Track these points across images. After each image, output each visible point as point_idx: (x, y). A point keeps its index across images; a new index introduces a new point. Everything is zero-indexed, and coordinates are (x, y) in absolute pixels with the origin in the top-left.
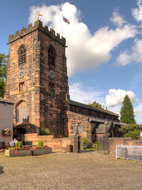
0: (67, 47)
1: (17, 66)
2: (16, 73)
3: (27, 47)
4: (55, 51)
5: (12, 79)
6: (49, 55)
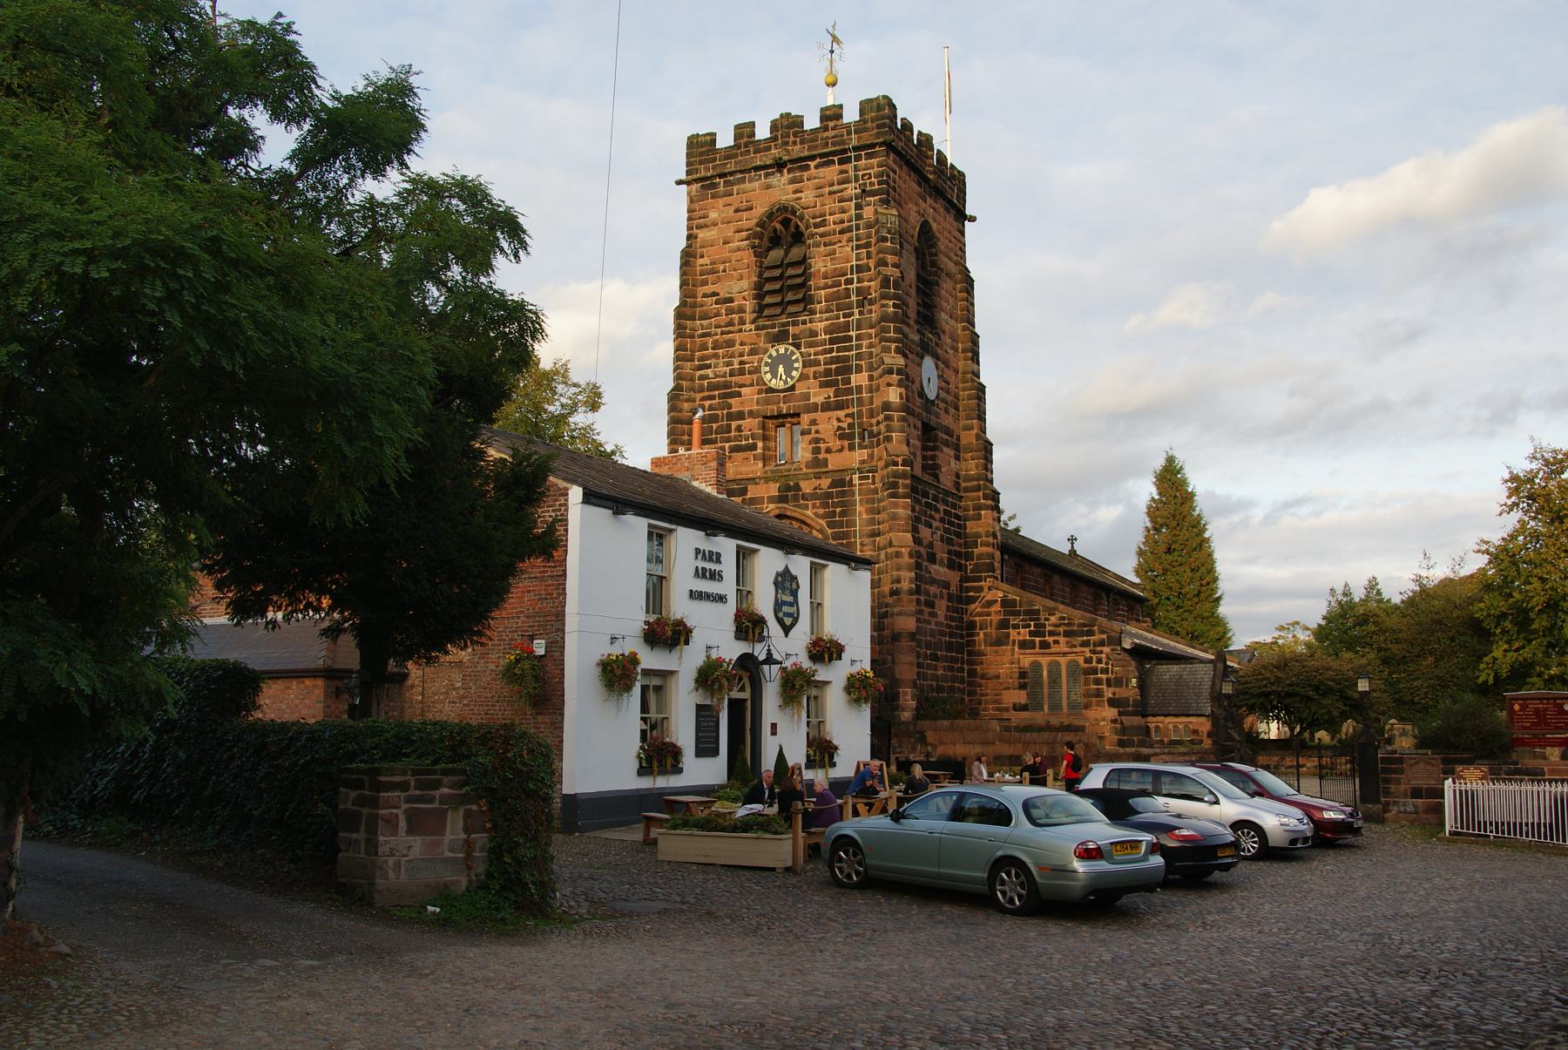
0: (973, 219)
1: (748, 317)
2: (741, 355)
3: (816, 226)
4: (934, 250)
5: (712, 387)
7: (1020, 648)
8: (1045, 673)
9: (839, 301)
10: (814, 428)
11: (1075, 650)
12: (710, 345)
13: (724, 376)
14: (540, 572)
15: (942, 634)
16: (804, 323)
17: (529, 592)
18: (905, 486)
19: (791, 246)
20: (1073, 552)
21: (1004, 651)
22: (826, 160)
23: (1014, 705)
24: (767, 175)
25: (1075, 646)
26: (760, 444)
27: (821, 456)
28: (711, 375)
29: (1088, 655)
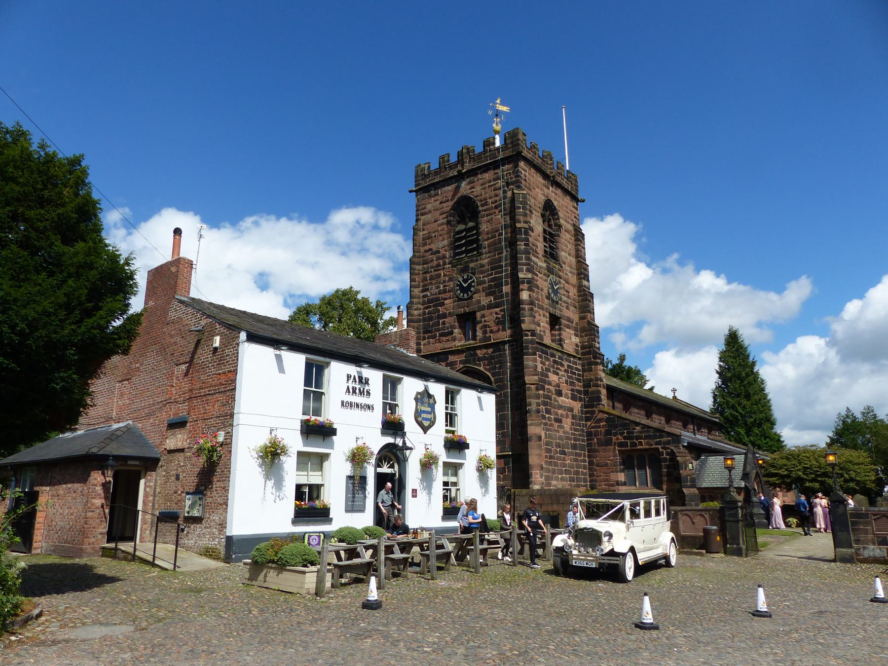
5: (430, 301)
6: (545, 231)
8: (635, 462)
12: (428, 278)
13: (436, 294)
14: (224, 388)
15: (568, 438)
17: (218, 401)
18: (533, 348)
20: (675, 397)
22: (485, 169)
27: (487, 335)
28: (429, 294)
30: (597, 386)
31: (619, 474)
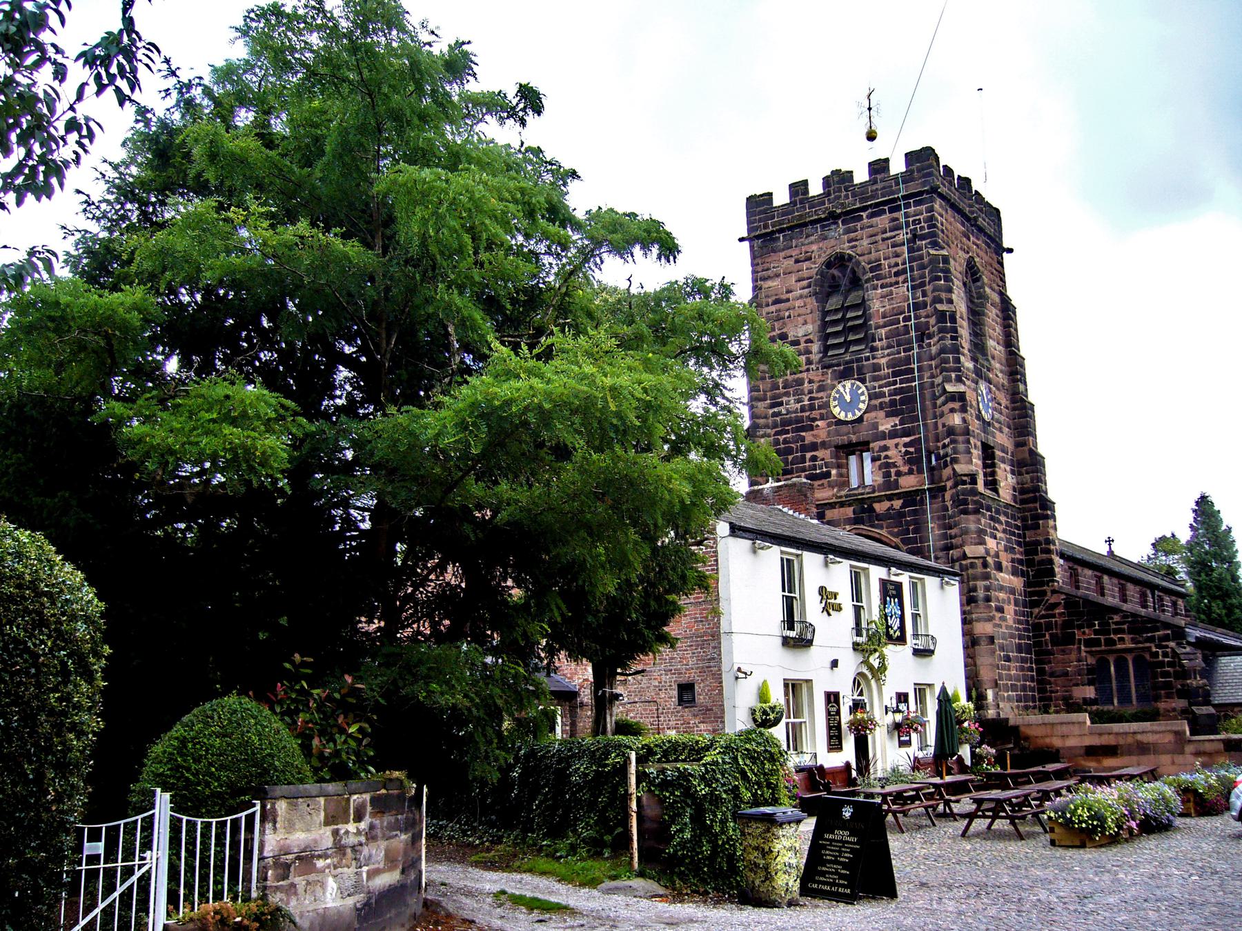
0: (1010, 251)
1: (815, 357)
4: (979, 284)
5: (785, 423)
7: (1085, 646)
8: (1112, 669)
9: (899, 339)
10: (883, 454)
11: (1141, 645)
13: (796, 412)
15: (1012, 636)
16: (867, 359)
19: (849, 291)
20: (1111, 552)
21: (1071, 650)
23: (1084, 699)
24: (823, 227)
25: (1140, 642)
26: (834, 472)
28: (784, 412)
29: (1154, 649)
30: (1049, 551)
31: (1087, 687)
